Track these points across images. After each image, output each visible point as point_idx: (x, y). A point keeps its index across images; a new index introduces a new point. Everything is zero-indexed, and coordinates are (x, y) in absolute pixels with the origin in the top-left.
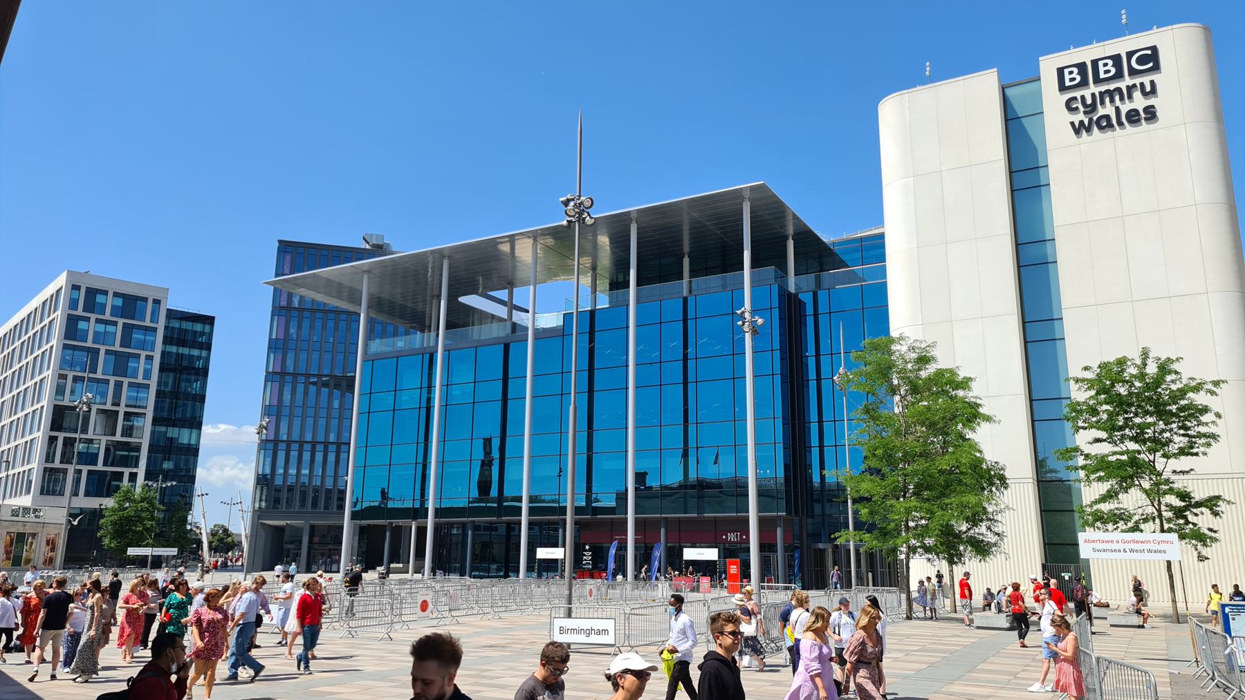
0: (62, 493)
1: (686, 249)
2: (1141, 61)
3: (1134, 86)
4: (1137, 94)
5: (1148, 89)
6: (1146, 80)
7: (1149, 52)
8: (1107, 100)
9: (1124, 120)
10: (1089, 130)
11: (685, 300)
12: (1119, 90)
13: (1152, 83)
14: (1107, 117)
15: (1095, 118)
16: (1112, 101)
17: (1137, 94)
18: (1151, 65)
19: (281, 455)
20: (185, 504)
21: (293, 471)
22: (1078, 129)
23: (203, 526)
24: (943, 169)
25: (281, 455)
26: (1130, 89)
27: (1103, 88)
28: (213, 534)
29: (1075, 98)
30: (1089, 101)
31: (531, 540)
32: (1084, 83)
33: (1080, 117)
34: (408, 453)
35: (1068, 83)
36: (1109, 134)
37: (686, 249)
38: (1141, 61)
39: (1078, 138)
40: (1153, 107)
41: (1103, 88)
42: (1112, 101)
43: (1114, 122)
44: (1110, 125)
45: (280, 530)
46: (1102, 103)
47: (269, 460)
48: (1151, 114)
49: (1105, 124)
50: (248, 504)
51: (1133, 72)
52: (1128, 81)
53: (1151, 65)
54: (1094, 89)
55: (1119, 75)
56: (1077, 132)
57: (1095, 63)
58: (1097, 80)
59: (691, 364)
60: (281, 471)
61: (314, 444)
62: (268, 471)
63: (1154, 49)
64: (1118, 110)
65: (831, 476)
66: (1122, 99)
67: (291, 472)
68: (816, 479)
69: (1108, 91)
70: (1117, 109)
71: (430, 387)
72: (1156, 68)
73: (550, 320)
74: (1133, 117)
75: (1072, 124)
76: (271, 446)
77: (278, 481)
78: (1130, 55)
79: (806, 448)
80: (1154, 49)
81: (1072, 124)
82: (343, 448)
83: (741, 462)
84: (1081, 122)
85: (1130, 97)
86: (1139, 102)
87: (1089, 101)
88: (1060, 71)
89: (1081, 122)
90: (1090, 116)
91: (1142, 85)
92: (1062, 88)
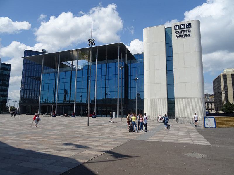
1: (107, 55)
2: (188, 26)
4: (187, 32)
6: (189, 29)
11: (106, 64)
12: (184, 30)
14: (182, 35)
17: (187, 32)
19: (25, 92)
20: (5, 101)
21: (28, 95)
22: (178, 37)
23: (9, 107)
25: (25, 92)
28: (11, 108)
32: (179, 29)
33: (178, 35)
34: (52, 92)
35: (176, 29)
37: (107, 55)
38: (188, 26)
42: (183, 32)
45: (26, 106)
46: (182, 32)
47: (23, 93)
48: (189, 35)
49: (182, 36)
50: (18, 102)
51: (187, 28)
52: (186, 29)
54: (180, 30)
55: (184, 28)
56: (177, 37)
57: (181, 25)
58: (181, 28)
59: (107, 76)
60: (25, 95)
61: (32, 90)
62: (23, 95)
63: (190, 24)
65: (132, 98)
66: (185, 32)
67: (29, 95)
68: (129, 98)
69: (183, 30)
71: (56, 79)
72: (191, 27)
73: (80, 67)
74: (186, 35)
76: (23, 90)
77: (25, 97)
78: (186, 24)
79: (128, 92)
80: (190, 24)
82: (38, 91)
83: (116, 95)
86: (188, 33)
88: (175, 26)
92: (175, 29)
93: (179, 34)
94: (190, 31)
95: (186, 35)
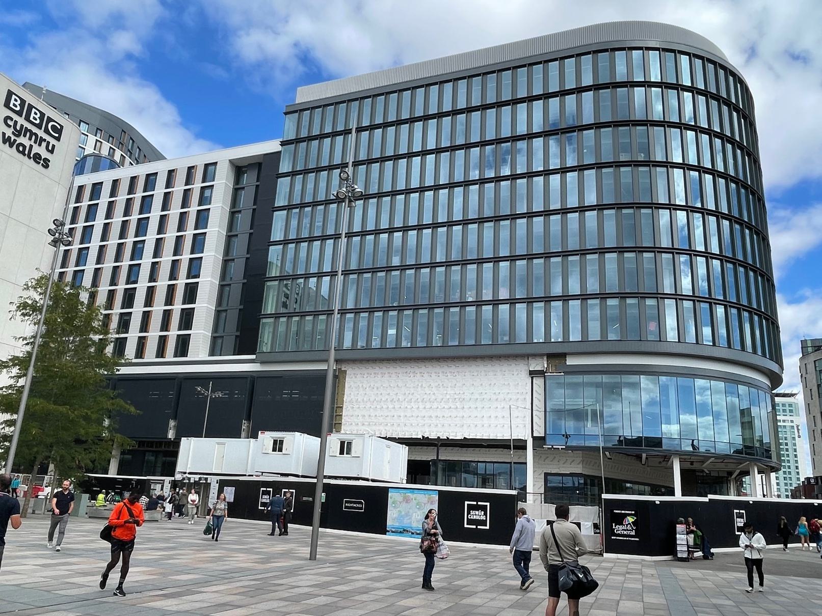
3: (45, 140)
4: (44, 144)
5: (50, 148)
6: (53, 141)
7: (59, 127)
8: (28, 134)
9: (32, 156)
10: (11, 146)
12: (36, 135)
13: (54, 146)
14: (24, 147)
17: (44, 144)
18: (57, 135)
26: (42, 140)
29: (12, 119)
30: (18, 128)
33: (9, 132)
36: (21, 156)
39: (3, 144)
40: (49, 161)
41: (27, 125)
42: (30, 139)
43: (26, 153)
44: (23, 153)
46: (25, 136)
49: (22, 150)
51: (47, 131)
53: (57, 135)
55: (39, 126)
56: (4, 142)
58: (27, 119)
64: (31, 146)
66: (35, 142)
69: (30, 131)
70: (31, 146)
74: (37, 158)
75: (4, 134)
81: (4, 134)
84: (9, 138)
85: (40, 145)
86: (42, 150)
87: (18, 128)
89: (9, 138)
90: (16, 138)
92: (7, 105)
93: (18, 133)
94: (52, 152)
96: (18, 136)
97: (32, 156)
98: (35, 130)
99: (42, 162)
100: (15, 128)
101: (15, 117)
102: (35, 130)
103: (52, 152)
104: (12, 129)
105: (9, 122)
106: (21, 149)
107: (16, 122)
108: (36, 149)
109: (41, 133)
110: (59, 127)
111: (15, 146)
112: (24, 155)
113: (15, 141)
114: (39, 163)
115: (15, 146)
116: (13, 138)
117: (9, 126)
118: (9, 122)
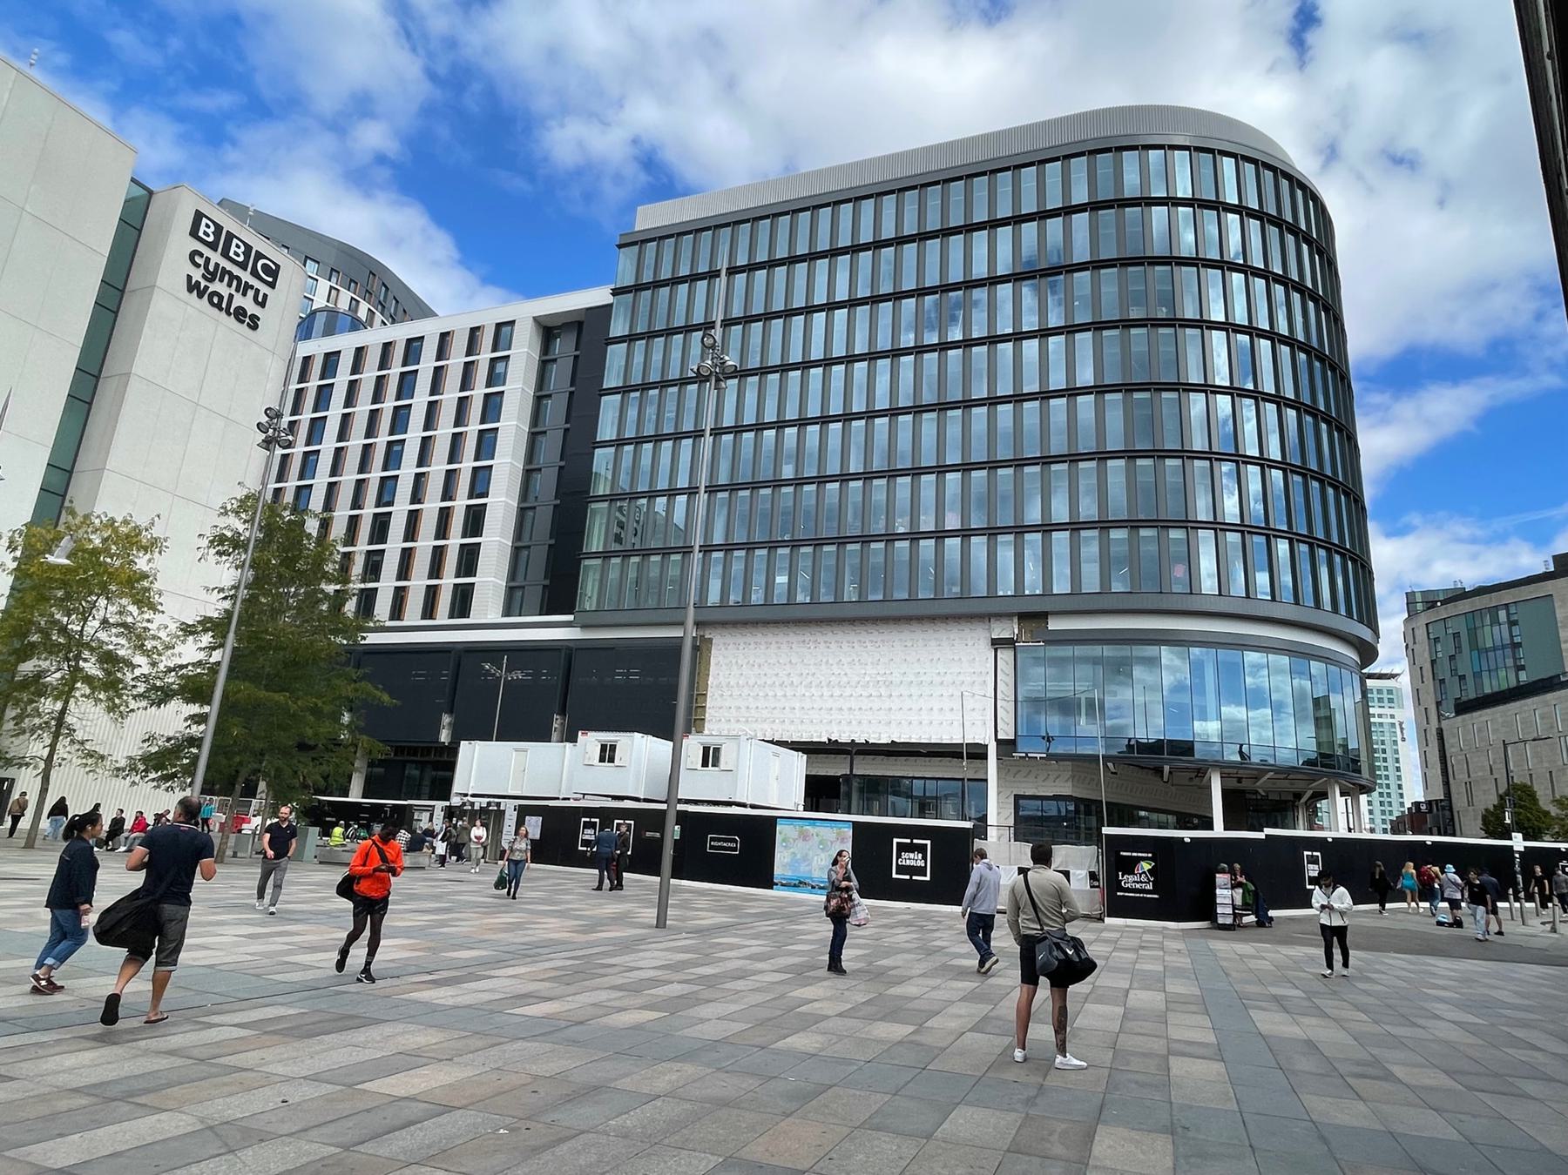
0: (564, 347)
3: (252, 287)
4: (251, 293)
5: (260, 300)
6: (264, 289)
7: (274, 267)
9: (232, 311)
10: (200, 296)
12: (239, 279)
13: (265, 296)
14: (221, 297)
15: (210, 290)
16: (230, 285)
17: (251, 293)
18: (270, 279)
22: (192, 287)
24: (28, 208)
26: (248, 286)
27: (225, 263)
29: (201, 255)
30: (211, 268)
31: (234, 665)
32: (213, 246)
33: (197, 275)
36: (216, 310)
40: (259, 319)
41: (225, 263)
42: (230, 285)
43: (224, 306)
44: (219, 306)
46: (221, 280)
48: (254, 323)
49: (217, 302)
51: (255, 273)
53: (270, 279)
54: (216, 257)
55: (243, 266)
56: (190, 290)
58: (225, 254)
64: (231, 296)
66: (237, 290)
69: (230, 273)
70: (231, 296)
72: (272, 285)
74: (240, 314)
75: (189, 278)
81: (189, 278)
84: (198, 283)
85: (244, 294)
86: (247, 303)
87: (211, 268)
89: (198, 283)
91: (257, 291)
92: (194, 233)
93: (211, 276)
94: (263, 305)
95: (240, 314)
96: (211, 280)
97: (232, 311)
98: (236, 271)
99: (247, 320)
100: (206, 268)
101: (207, 252)
102: (236, 271)
103: (263, 305)
104: (202, 270)
105: (198, 260)
106: (216, 300)
107: (208, 260)
108: (239, 301)
109: (246, 276)
110: (274, 267)
111: (206, 296)
112: (221, 309)
113: (206, 288)
114: (243, 322)
115: (206, 296)
116: (203, 283)
117: (198, 266)
118: (198, 260)
